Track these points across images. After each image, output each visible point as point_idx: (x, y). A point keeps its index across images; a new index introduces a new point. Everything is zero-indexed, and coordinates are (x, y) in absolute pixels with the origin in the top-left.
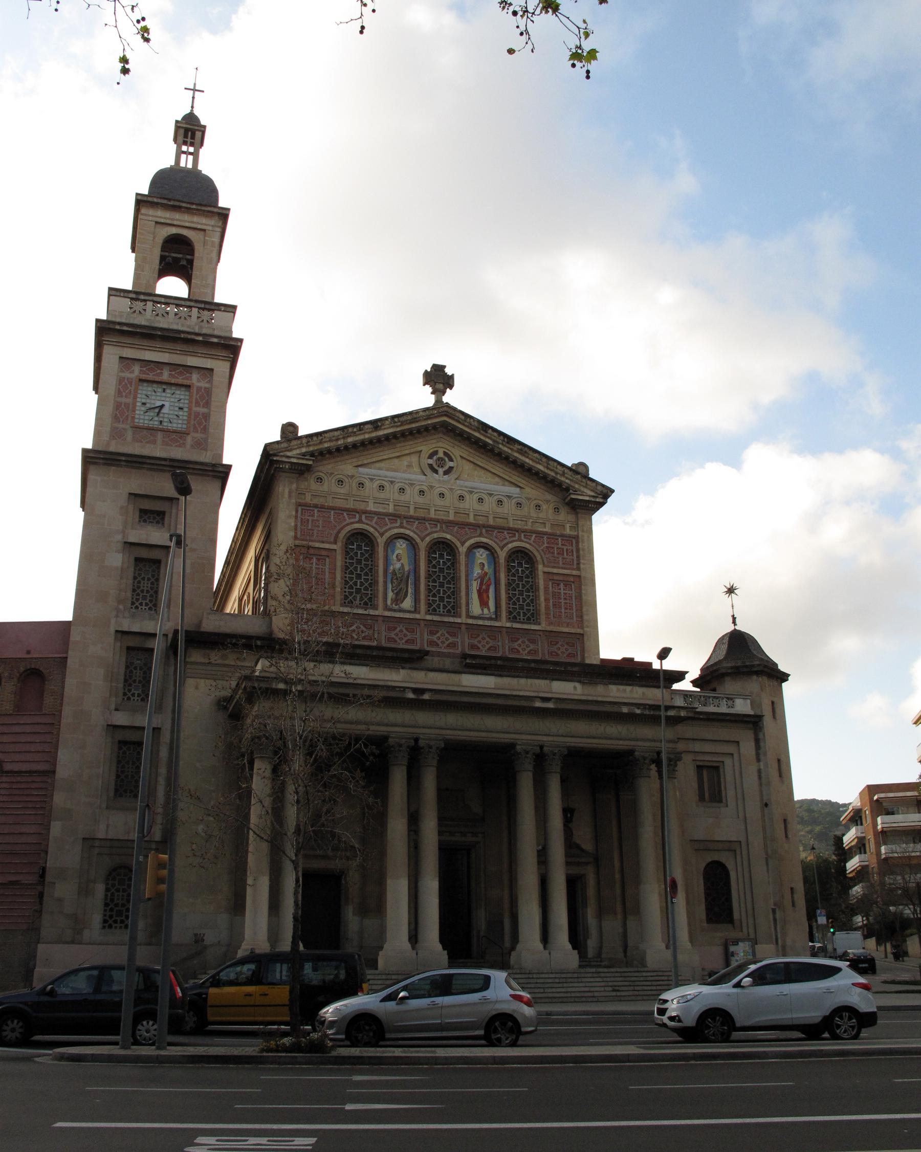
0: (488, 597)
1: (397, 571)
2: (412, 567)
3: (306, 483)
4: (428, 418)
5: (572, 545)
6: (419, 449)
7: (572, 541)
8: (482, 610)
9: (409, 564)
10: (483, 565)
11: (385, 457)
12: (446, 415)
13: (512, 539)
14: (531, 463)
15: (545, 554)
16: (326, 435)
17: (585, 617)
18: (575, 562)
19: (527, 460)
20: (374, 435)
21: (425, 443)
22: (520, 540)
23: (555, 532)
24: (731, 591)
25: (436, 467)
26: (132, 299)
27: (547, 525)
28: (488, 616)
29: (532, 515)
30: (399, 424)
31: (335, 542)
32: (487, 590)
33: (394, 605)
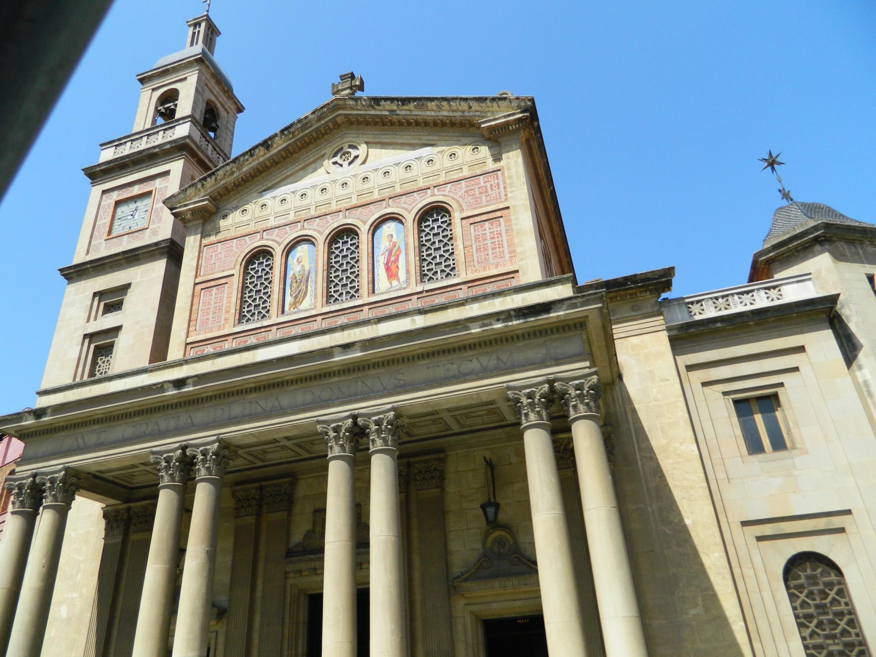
0: (397, 267)
1: (296, 275)
2: (312, 265)
3: (212, 224)
4: (320, 119)
5: (497, 179)
6: (323, 152)
7: (497, 175)
8: (391, 283)
9: (310, 263)
10: (392, 235)
11: (289, 173)
12: (339, 109)
13: (421, 199)
14: (433, 114)
15: (463, 199)
16: (219, 172)
17: (518, 250)
18: (503, 194)
19: (428, 113)
20: (268, 155)
21: (329, 145)
22: (434, 195)
23: (474, 172)
25: (340, 162)
26: (117, 146)
27: (464, 170)
28: (398, 288)
29: (445, 166)
30: (291, 136)
31: (234, 268)
32: (397, 260)
33: (292, 309)
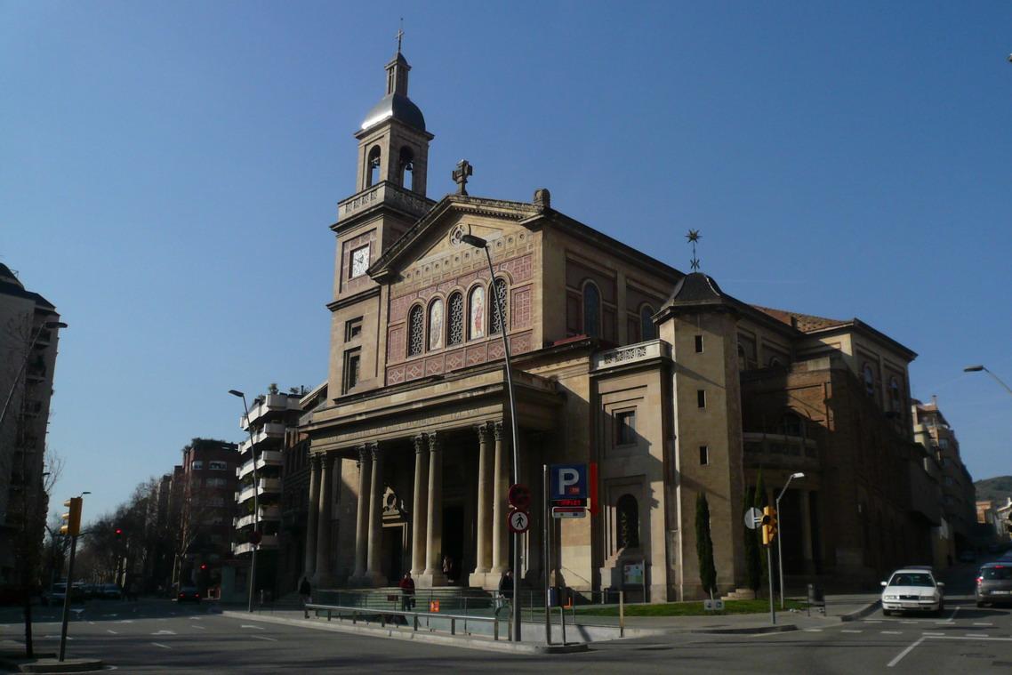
24: (694, 237)
